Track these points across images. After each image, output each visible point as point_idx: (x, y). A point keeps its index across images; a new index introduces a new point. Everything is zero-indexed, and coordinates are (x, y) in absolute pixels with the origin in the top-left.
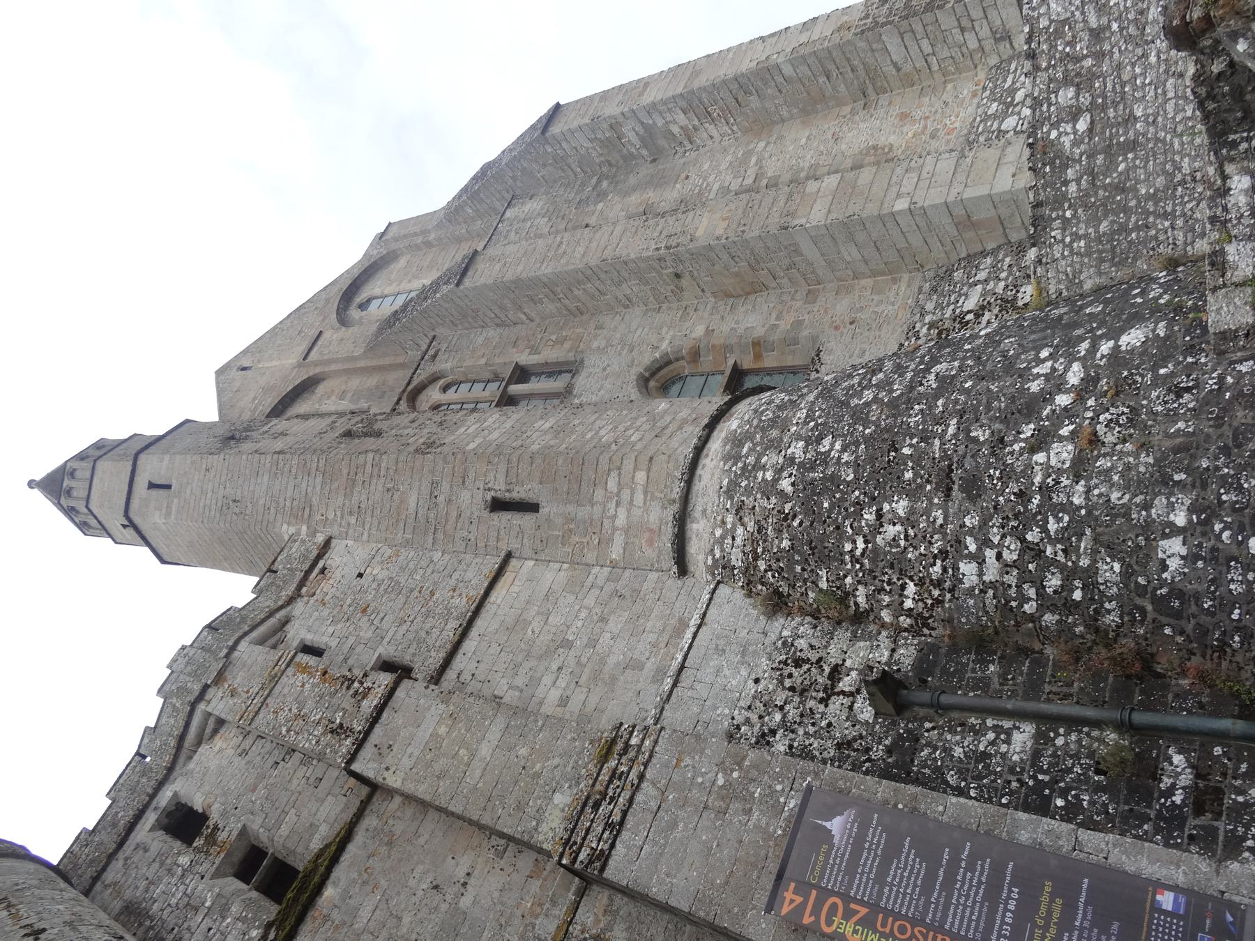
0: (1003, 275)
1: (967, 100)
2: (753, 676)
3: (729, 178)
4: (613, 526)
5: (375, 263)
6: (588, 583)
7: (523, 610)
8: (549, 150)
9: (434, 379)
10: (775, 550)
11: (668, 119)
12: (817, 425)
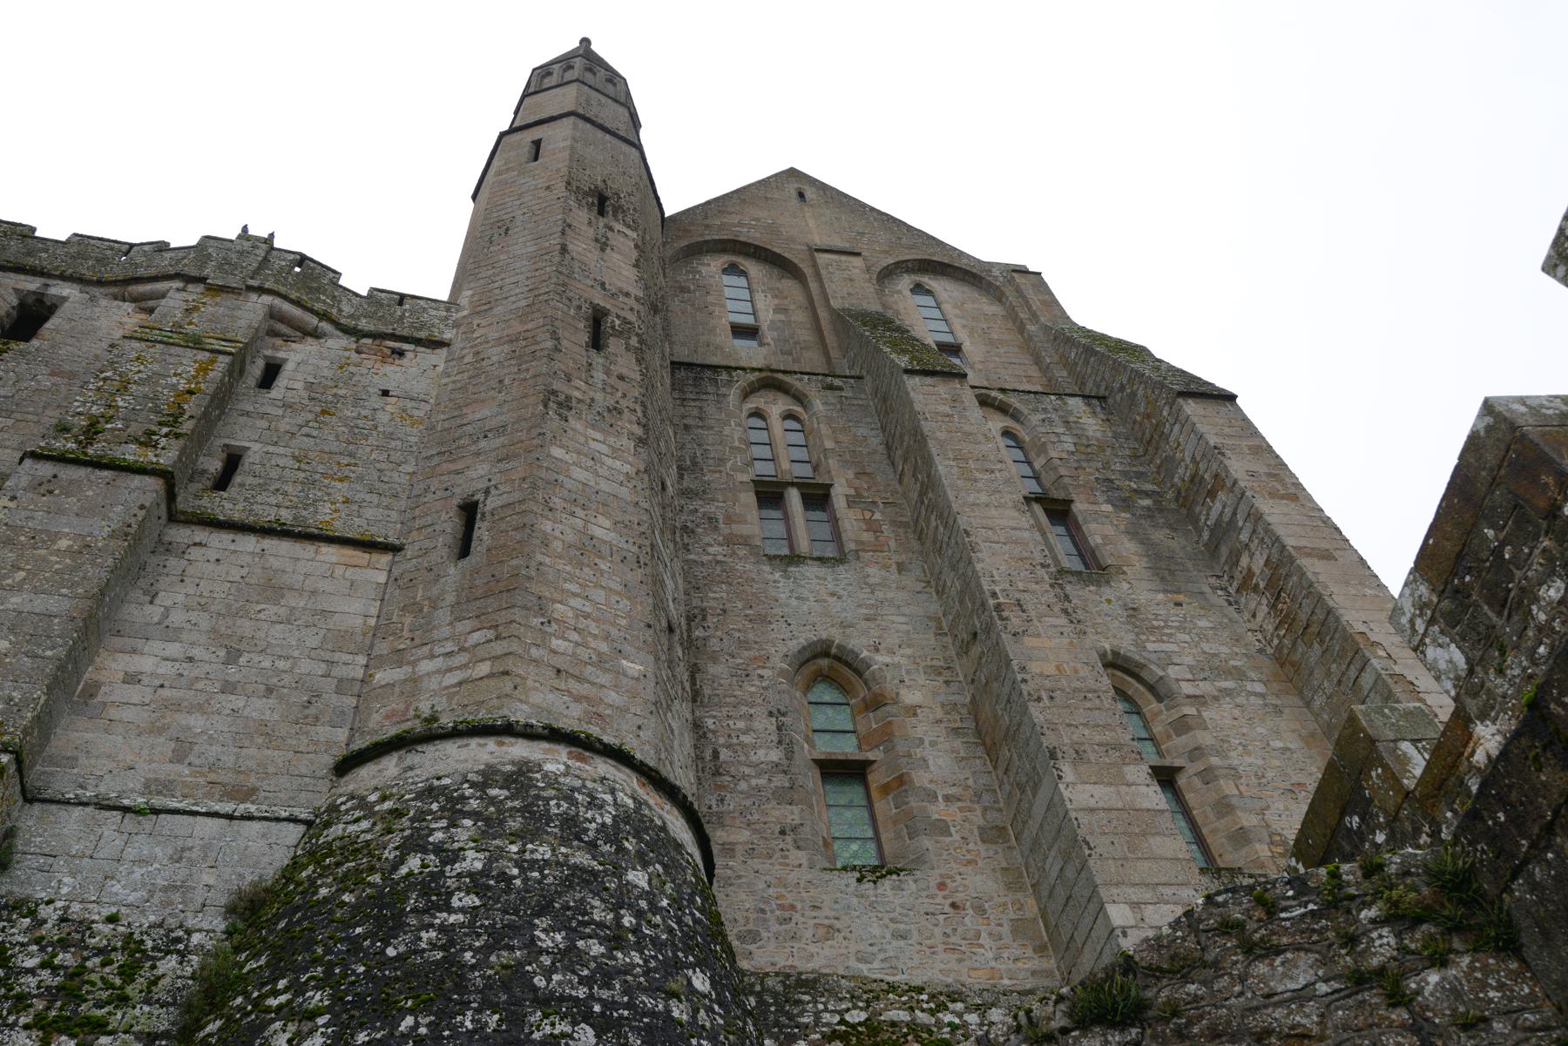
3: (1189, 660)
5: (981, 278)
8: (1165, 413)
9: (799, 398)
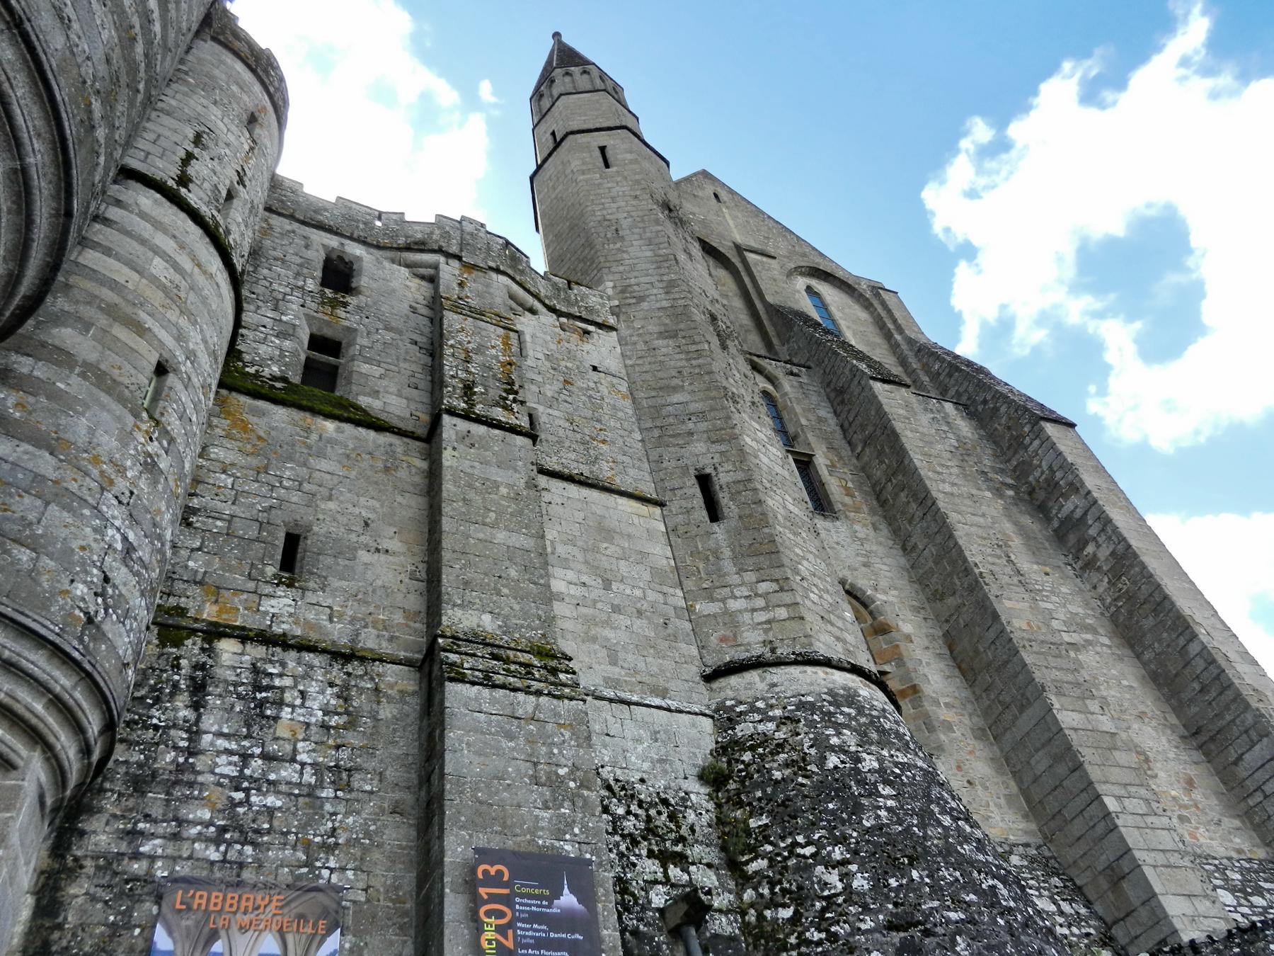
0: (1075, 930)
1: (1230, 845)
2: (645, 776)
3: (1062, 617)
4: (726, 599)
5: (855, 290)
6: (665, 589)
7: (621, 534)
8: (1026, 429)
10: (767, 766)
11: (1099, 539)
12: (897, 776)
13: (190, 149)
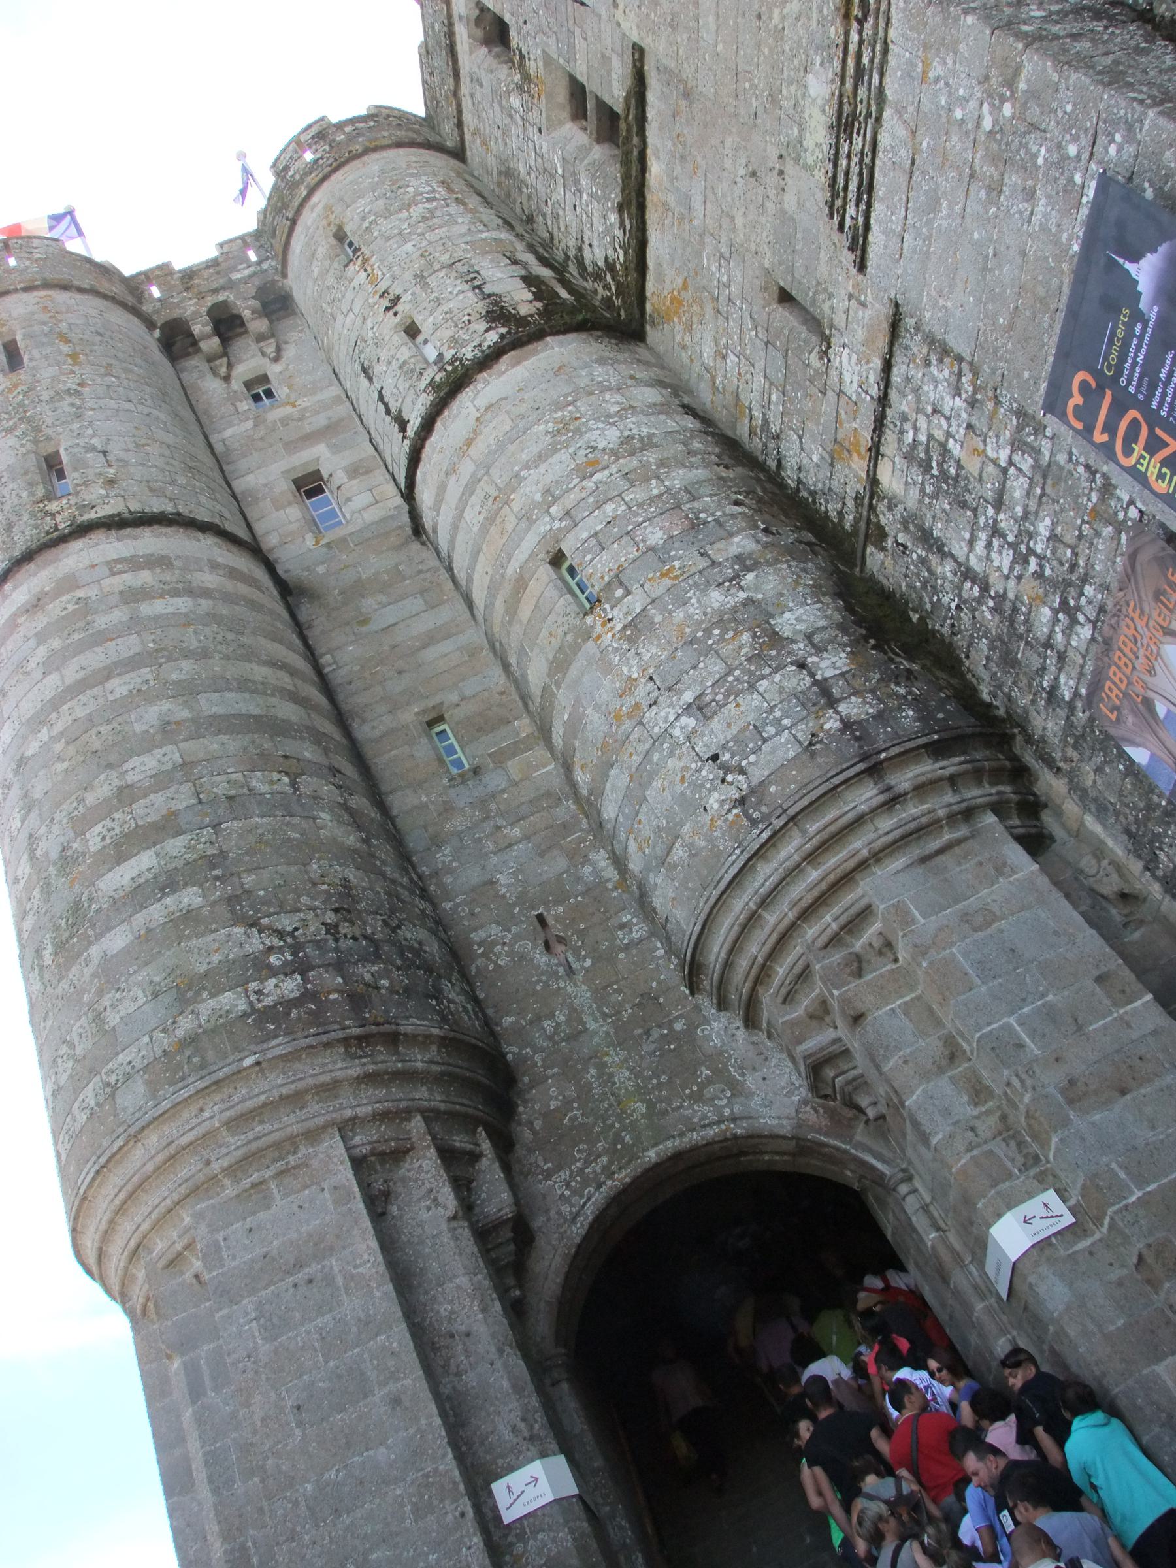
13: (376, 395)
